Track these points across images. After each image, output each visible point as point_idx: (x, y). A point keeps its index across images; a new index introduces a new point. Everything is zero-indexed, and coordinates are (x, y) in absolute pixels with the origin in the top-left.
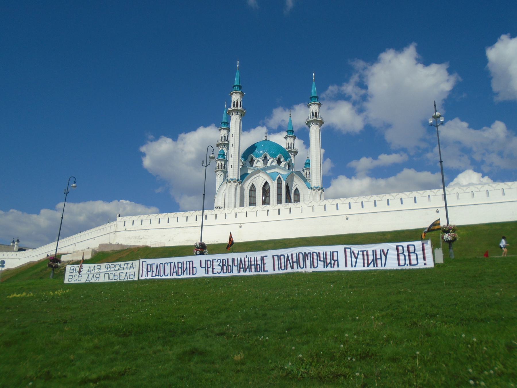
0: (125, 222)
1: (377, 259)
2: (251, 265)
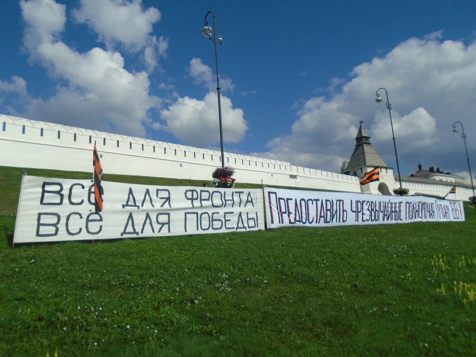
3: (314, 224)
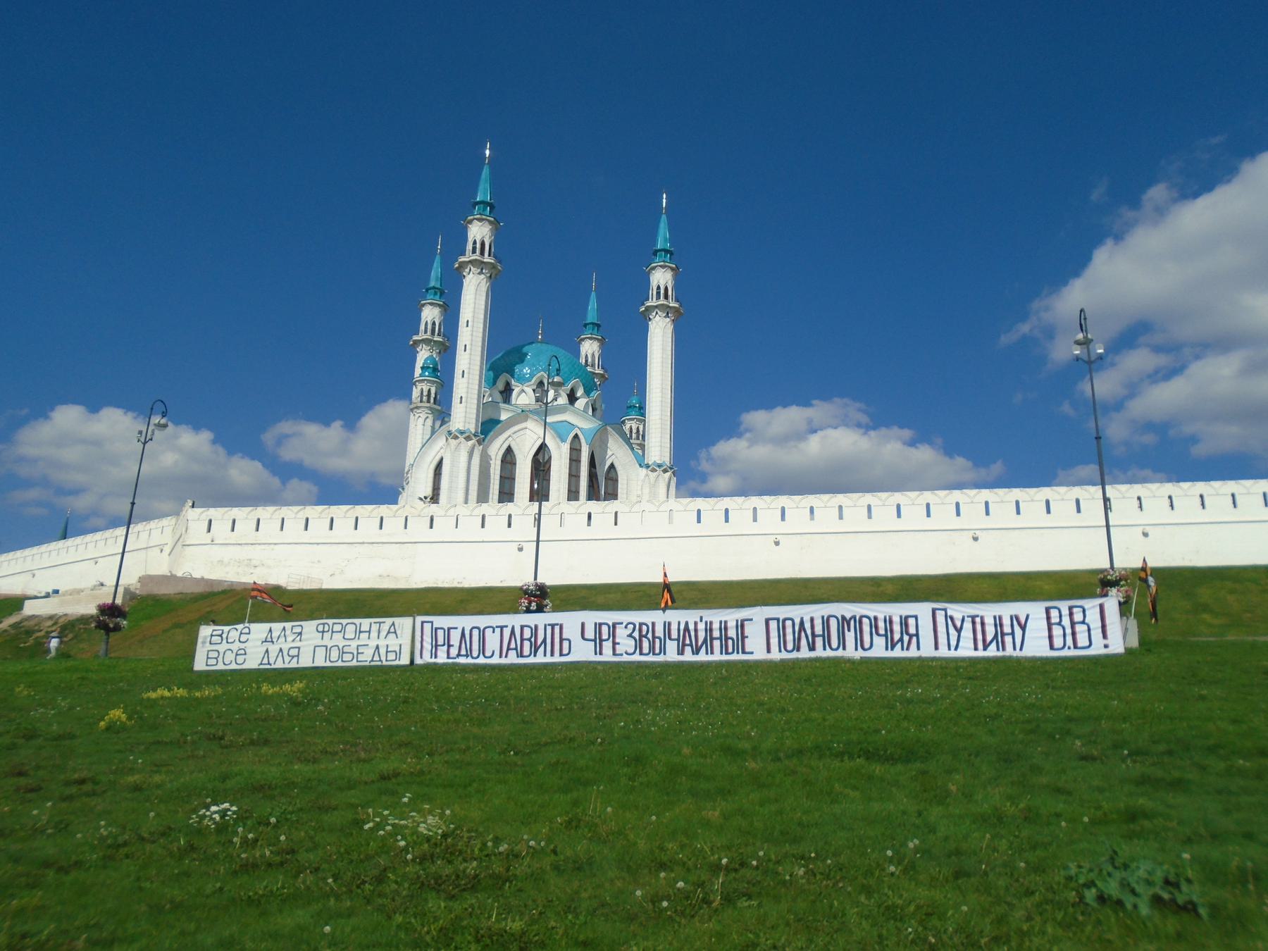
0: (210, 521)
1: (1003, 634)
2: (712, 639)
3: (496, 660)
